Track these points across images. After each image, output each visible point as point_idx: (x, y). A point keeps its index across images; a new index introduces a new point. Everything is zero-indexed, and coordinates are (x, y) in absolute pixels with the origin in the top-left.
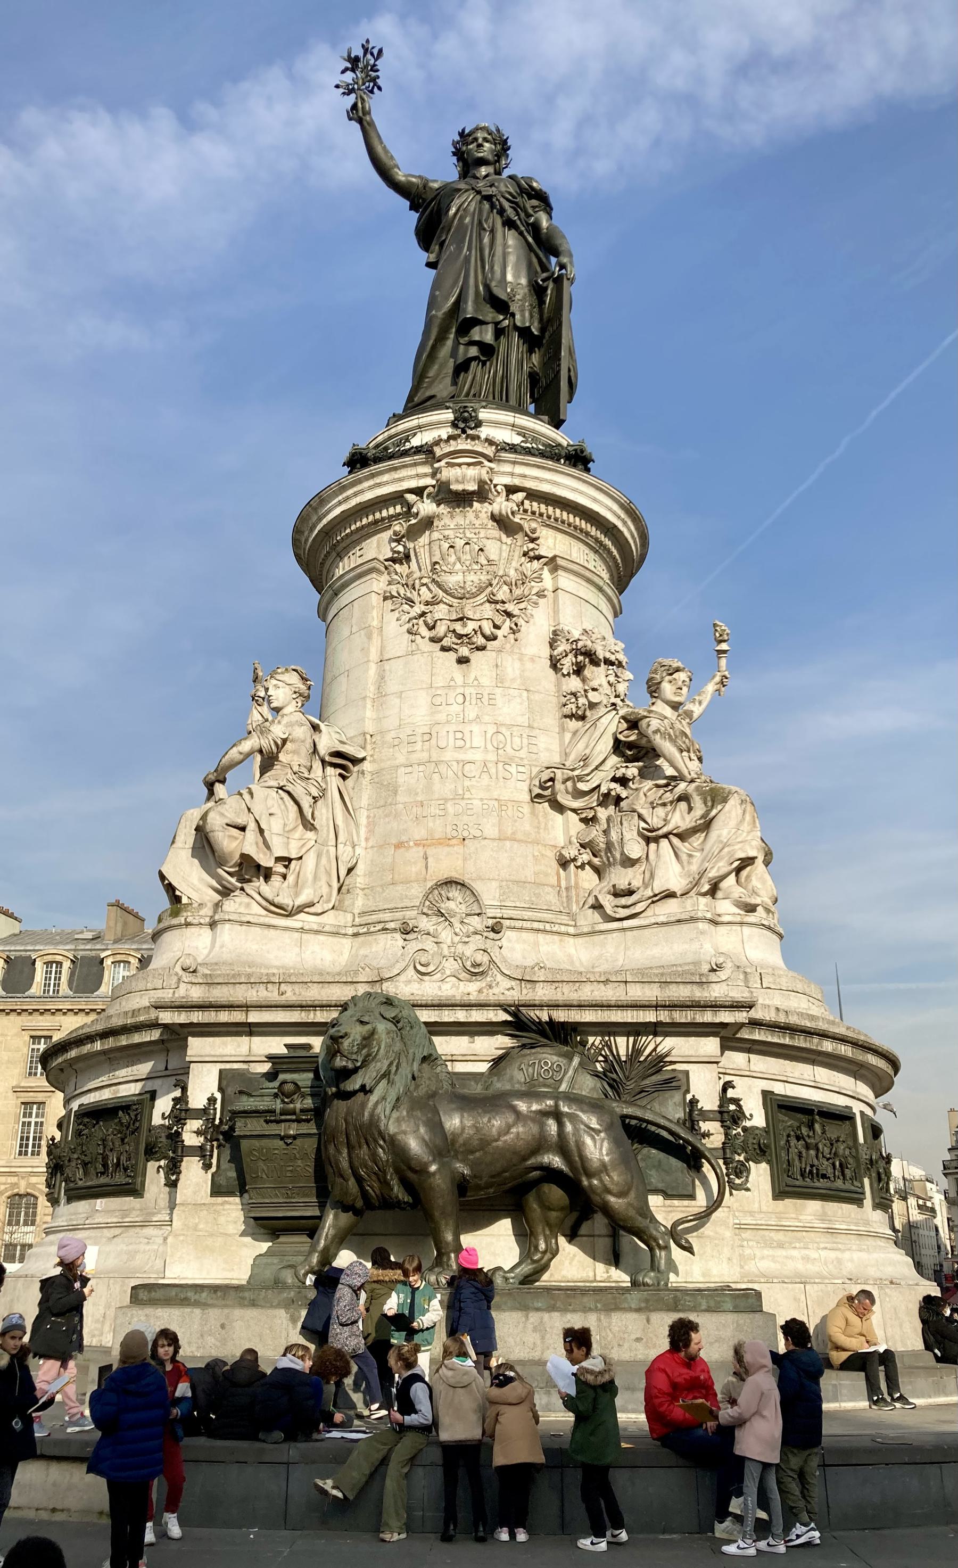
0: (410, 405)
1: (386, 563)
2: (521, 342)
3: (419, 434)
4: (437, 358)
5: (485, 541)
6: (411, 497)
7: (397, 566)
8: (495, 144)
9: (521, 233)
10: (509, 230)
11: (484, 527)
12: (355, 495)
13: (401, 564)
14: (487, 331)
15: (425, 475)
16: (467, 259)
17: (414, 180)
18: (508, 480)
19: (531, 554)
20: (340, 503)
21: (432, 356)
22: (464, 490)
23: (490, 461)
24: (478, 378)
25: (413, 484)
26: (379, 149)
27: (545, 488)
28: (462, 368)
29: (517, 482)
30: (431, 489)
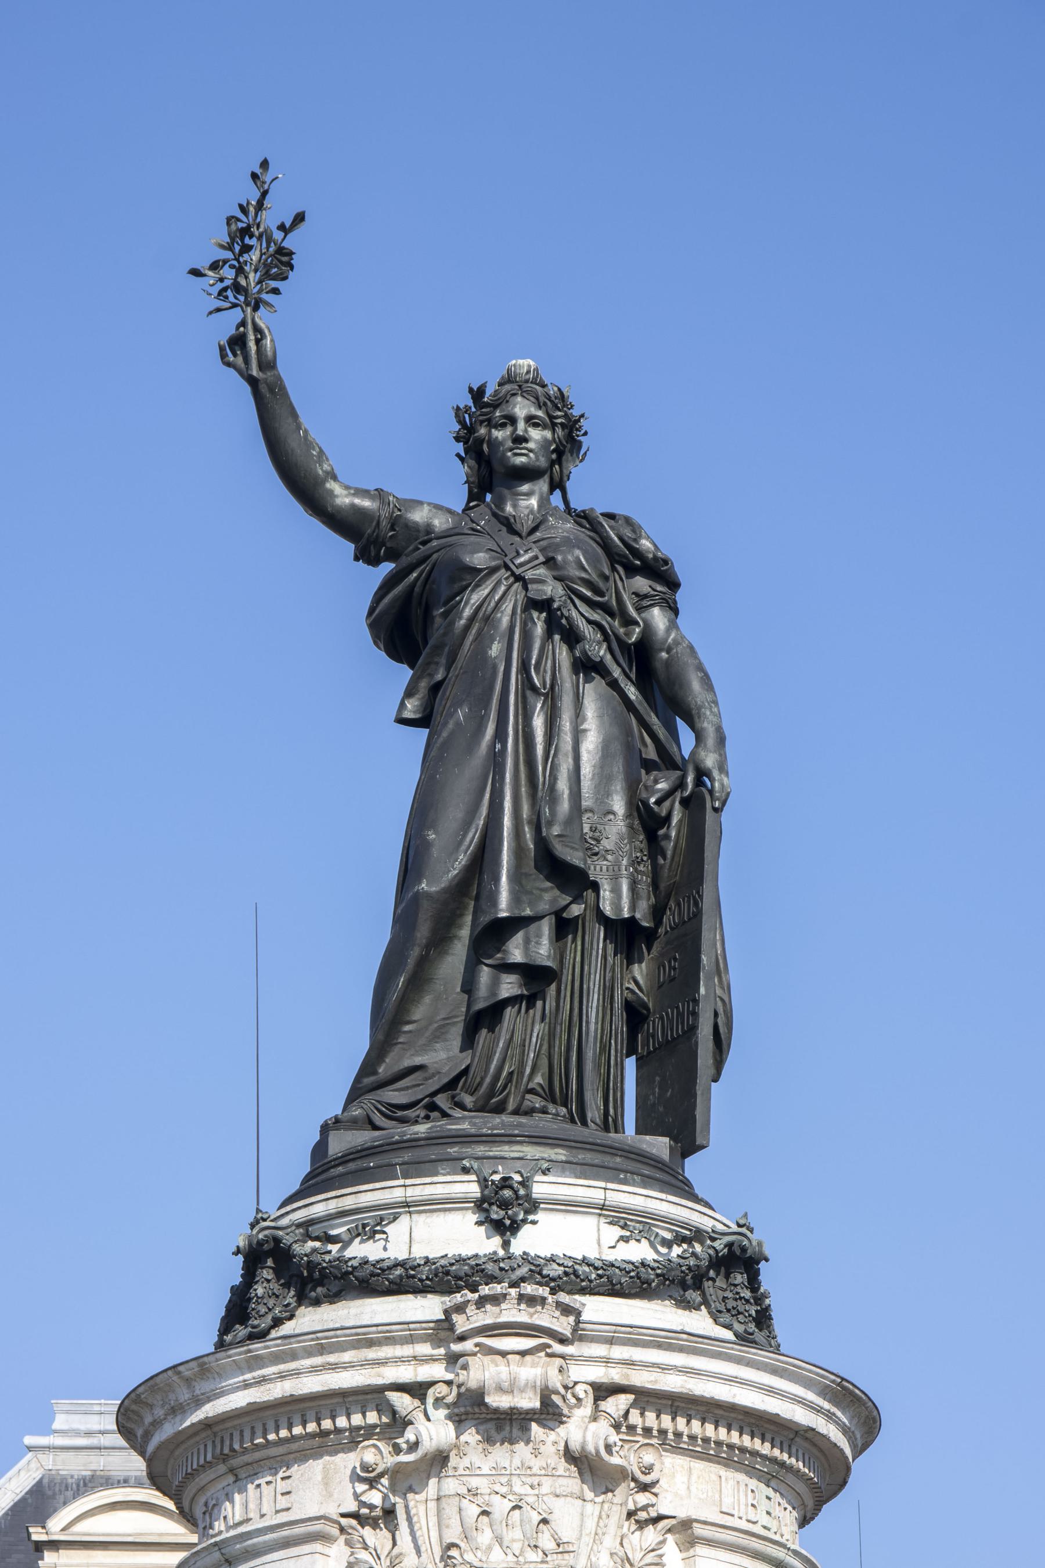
0: (368, 1081)
1: (344, 1521)
2: (610, 947)
3: (404, 1221)
4: (429, 980)
5: (550, 1500)
6: (402, 1402)
7: (367, 1532)
8: (553, 426)
9: (614, 684)
10: (587, 681)
11: (550, 1473)
12: (282, 1376)
13: (375, 1526)
14: (539, 936)
15: (433, 1359)
16: (496, 761)
17: (366, 503)
18: (598, 1374)
19: (643, 1515)
20: (246, 1386)
21: (419, 981)
22: (512, 1409)
23: (563, 1341)
24: (517, 1039)
25: (406, 1374)
26: (293, 443)
27: (672, 1383)
28: (484, 1019)
29: (615, 1375)
30: (442, 1389)
